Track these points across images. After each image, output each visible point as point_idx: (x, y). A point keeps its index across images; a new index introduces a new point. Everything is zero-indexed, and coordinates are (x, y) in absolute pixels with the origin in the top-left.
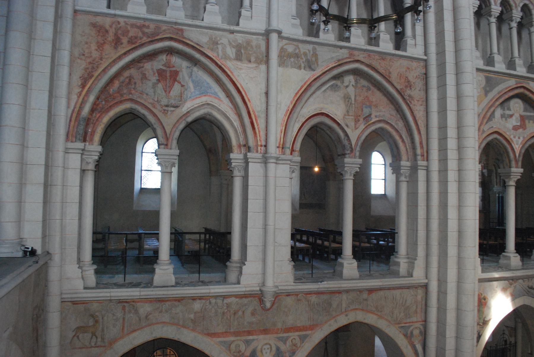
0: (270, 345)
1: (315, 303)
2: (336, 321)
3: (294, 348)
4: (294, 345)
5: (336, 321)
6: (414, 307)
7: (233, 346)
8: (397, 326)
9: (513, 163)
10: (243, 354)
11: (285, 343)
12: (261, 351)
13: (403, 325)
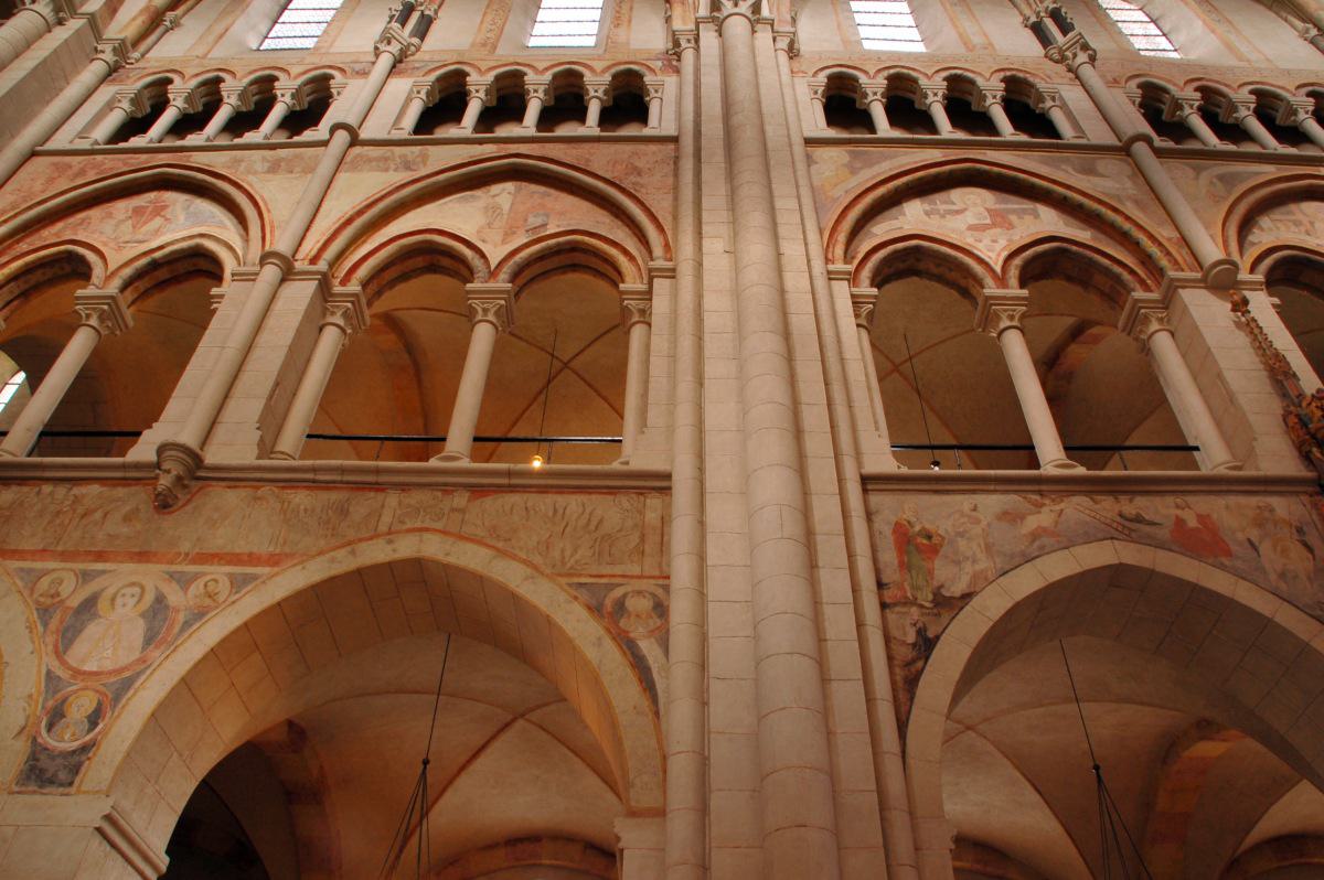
0: (143, 588)
1: (302, 507)
2: (353, 552)
3: (208, 601)
4: (210, 596)
5: (353, 552)
6: (635, 539)
7: (44, 583)
8: (564, 581)
9: (989, 281)
10: (62, 601)
11: (185, 589)
12: (113, 600)
13: (583, 580)
